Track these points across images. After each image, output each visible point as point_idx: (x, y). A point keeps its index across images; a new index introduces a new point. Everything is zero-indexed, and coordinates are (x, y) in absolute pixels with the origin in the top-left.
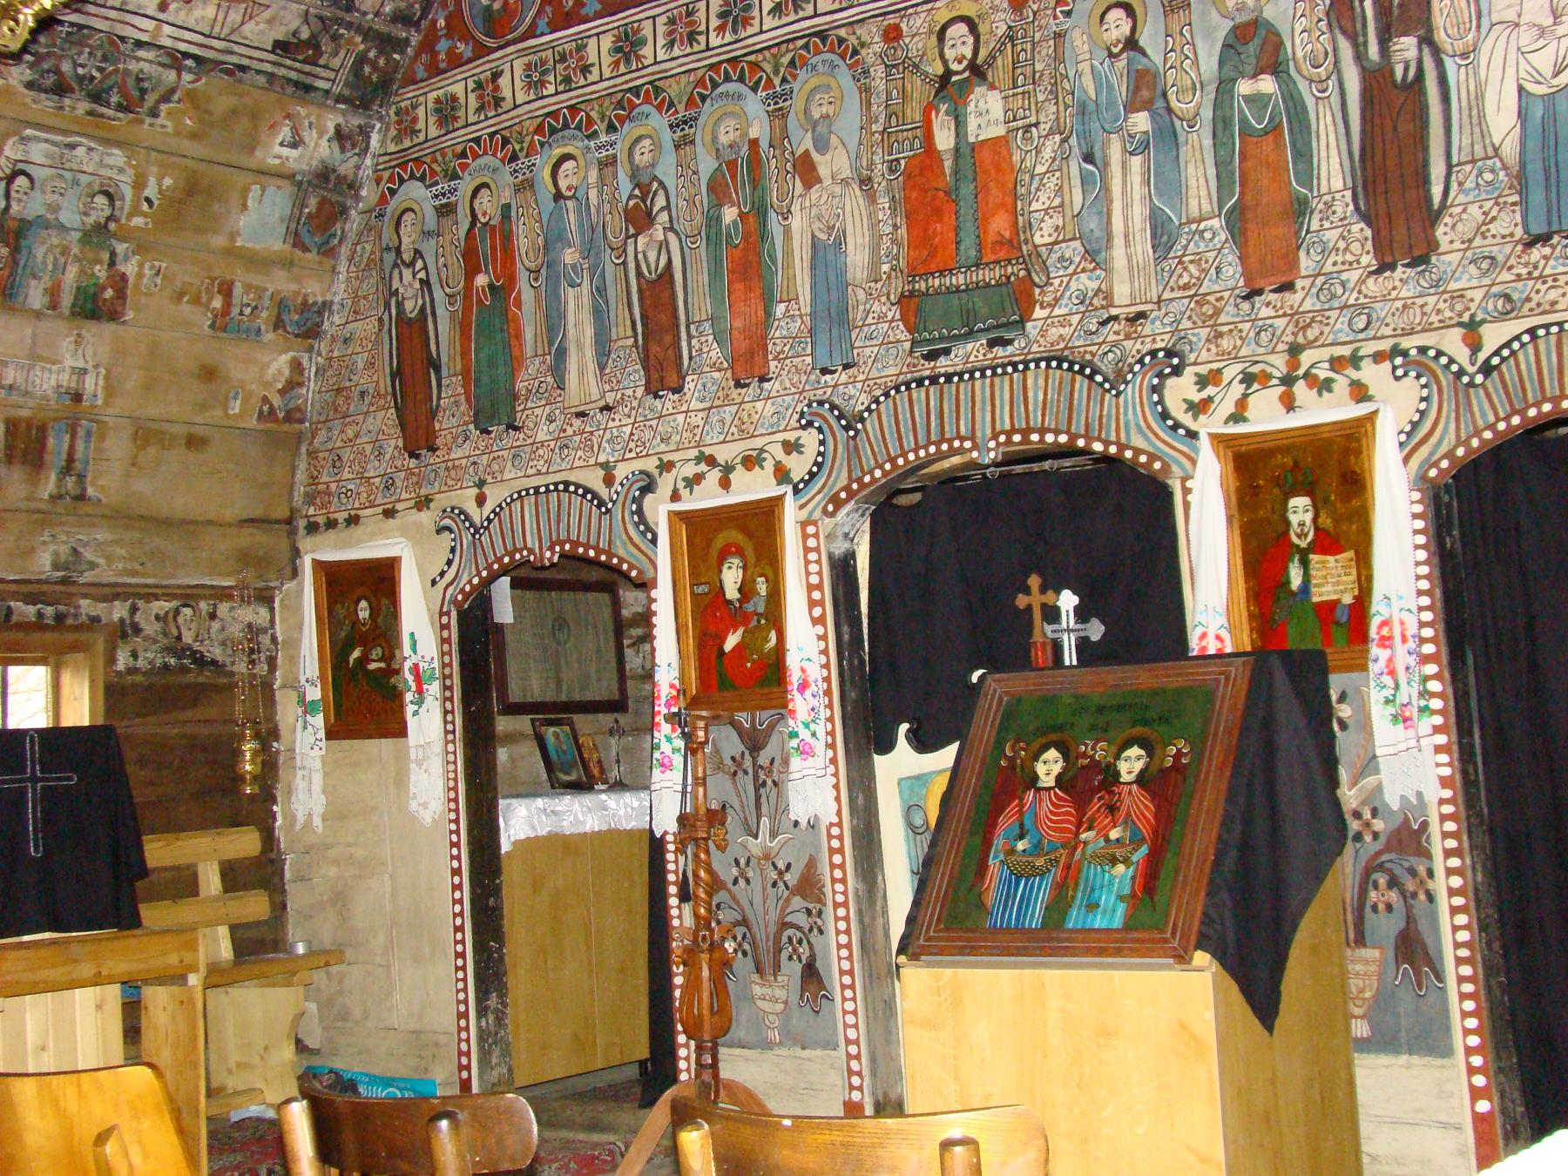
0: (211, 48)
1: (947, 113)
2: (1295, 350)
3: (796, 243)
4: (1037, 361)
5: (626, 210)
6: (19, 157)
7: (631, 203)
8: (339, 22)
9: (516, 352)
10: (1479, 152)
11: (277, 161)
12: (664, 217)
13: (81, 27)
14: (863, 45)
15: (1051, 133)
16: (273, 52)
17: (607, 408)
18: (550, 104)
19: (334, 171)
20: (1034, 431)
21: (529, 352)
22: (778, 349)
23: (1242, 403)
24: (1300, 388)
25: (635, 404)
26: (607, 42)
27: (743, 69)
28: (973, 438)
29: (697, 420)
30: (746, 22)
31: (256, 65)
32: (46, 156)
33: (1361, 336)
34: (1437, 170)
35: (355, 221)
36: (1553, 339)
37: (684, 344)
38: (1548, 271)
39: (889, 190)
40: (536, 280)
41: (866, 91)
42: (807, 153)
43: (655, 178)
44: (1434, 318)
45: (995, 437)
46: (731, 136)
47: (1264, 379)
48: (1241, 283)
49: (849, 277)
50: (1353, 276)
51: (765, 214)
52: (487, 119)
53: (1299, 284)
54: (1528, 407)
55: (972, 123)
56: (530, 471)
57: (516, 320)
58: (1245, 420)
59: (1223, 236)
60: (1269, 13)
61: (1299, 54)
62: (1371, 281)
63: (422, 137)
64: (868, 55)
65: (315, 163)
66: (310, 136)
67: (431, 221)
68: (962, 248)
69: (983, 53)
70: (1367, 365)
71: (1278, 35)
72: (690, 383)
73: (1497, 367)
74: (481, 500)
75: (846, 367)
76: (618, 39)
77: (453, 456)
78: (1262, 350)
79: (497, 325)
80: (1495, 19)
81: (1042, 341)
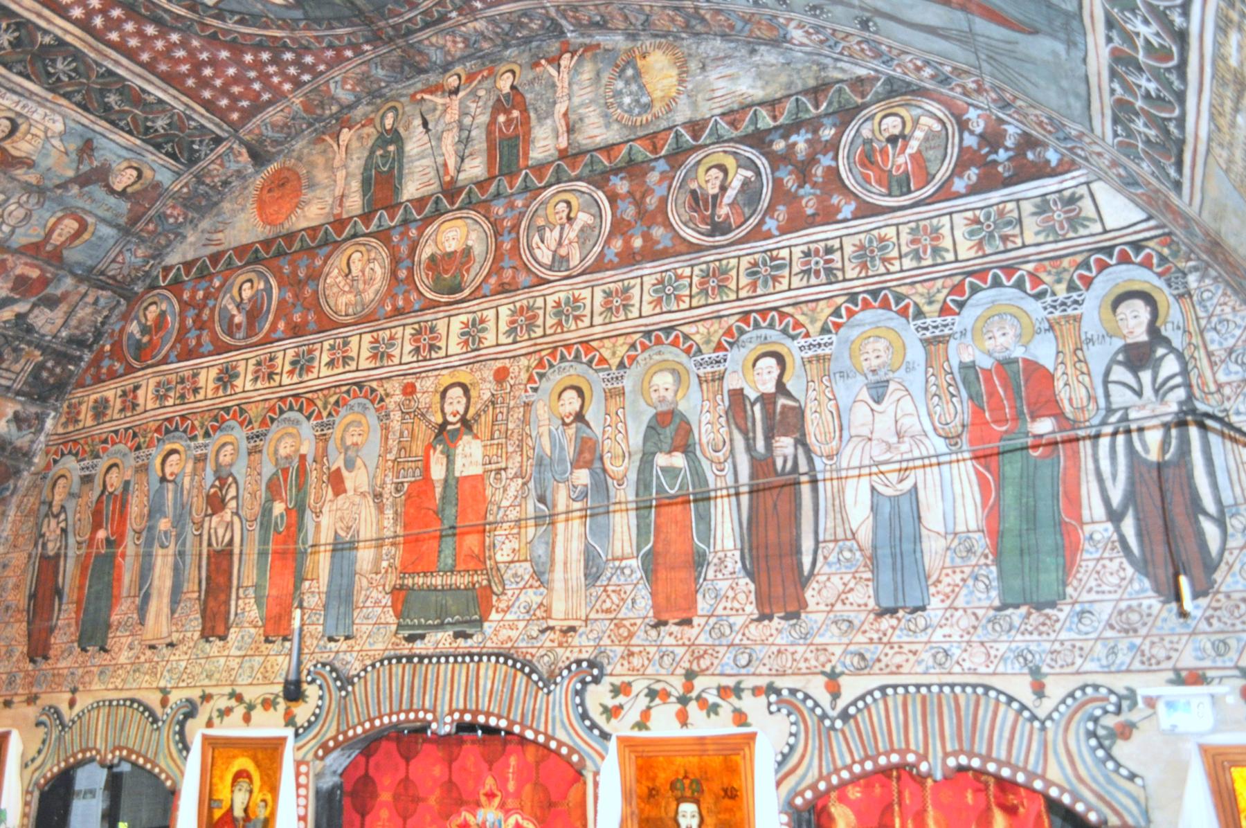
2: (690, 675)
4: (489, 655)
5: (208, 496)
8: (22, 340)
9: (115, 592)
10: (840, 535)
12: (233, 504)
14: (387, 395)
15: (516, 476)
17: (171, 645)
18: (168, 412)
20: (481, 713)
21: (124, 593)
23: (646, 714)
24: (693, 707)
26: (214, 373)
27: (301, 403)
28: (434, 712)
29: (234, 663)
30: (309, 370)
33: (743, 671)
34: (807, 544)
35: (26, 478)
36: (900, 699)
37: (233, 603)
38: (894, 639)
39: (394, 505)
41: (386, 428)
43: (231, 474)
44: (802, 665)
45: (451, 713)
47: (666, 695)
48: (651, 614)
49: (358, 567)
50: (739, 621)
51: (304, 512)
53: (696, 621)
54: (879, 754)
55: (459, 462)
57: (120, 567)
58: (647, 728)
59: (639, 574)
60: (682, 407)
61: (704, 440)
62: (752, 626)
63: (81, 425)
64: (391, 403)
69: (472, 412)
70: (747, 695)
71: (688, 423)
72: (233, 634)
73: (854, 717)
74: (72, 704)
75: (347, 638)
76: (221, 371)
78: (663, 671)
80: (853, 432)
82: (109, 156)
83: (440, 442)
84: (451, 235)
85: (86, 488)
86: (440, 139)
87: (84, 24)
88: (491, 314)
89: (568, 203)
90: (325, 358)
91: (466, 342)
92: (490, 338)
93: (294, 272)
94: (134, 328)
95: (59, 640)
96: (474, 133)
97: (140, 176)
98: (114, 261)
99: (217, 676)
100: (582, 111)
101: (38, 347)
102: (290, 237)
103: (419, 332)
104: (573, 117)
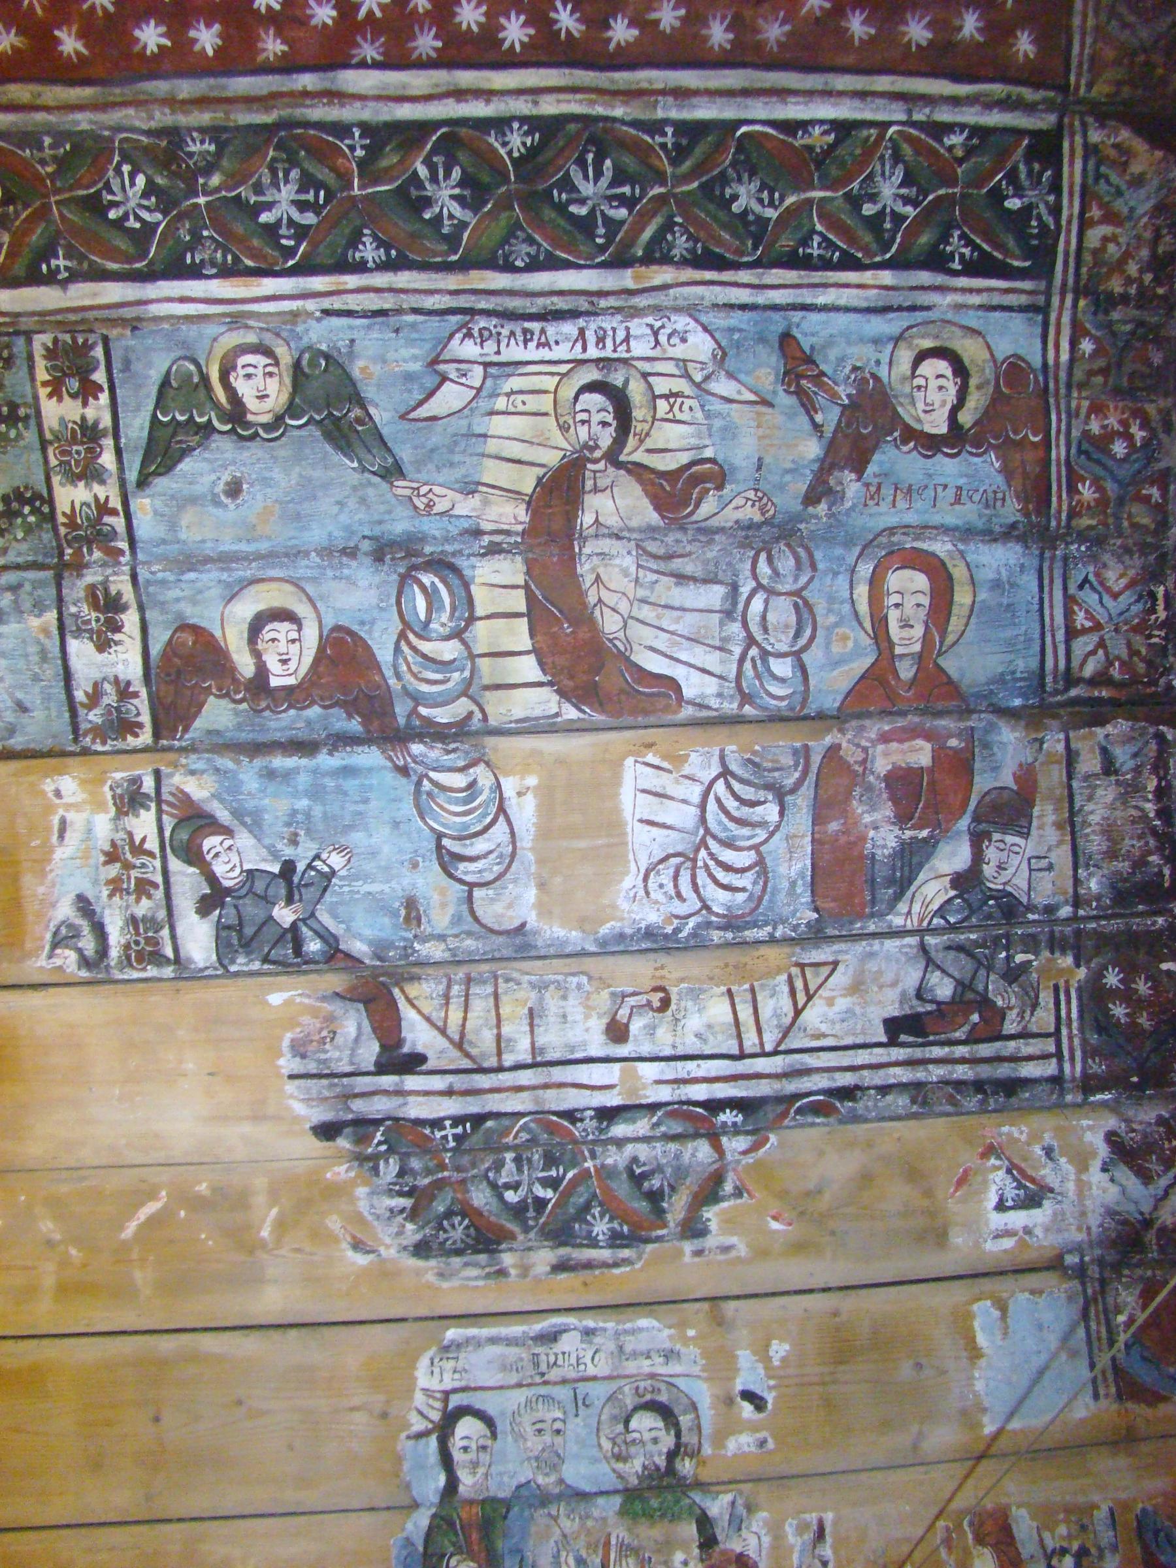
0: (758, 1076)
6: (448, 1384)
11: (1008, 1243)
13: (478, 1119)
16: (892, 1042)
31: (869, 1078)
32: (504, 1368)
65: (1094, 1221)
66: (1058, 1174)
82: (863, 354)
87: (549, 50)
97: (960, 370)
98: (1072, 633)
101: (1056, 944)
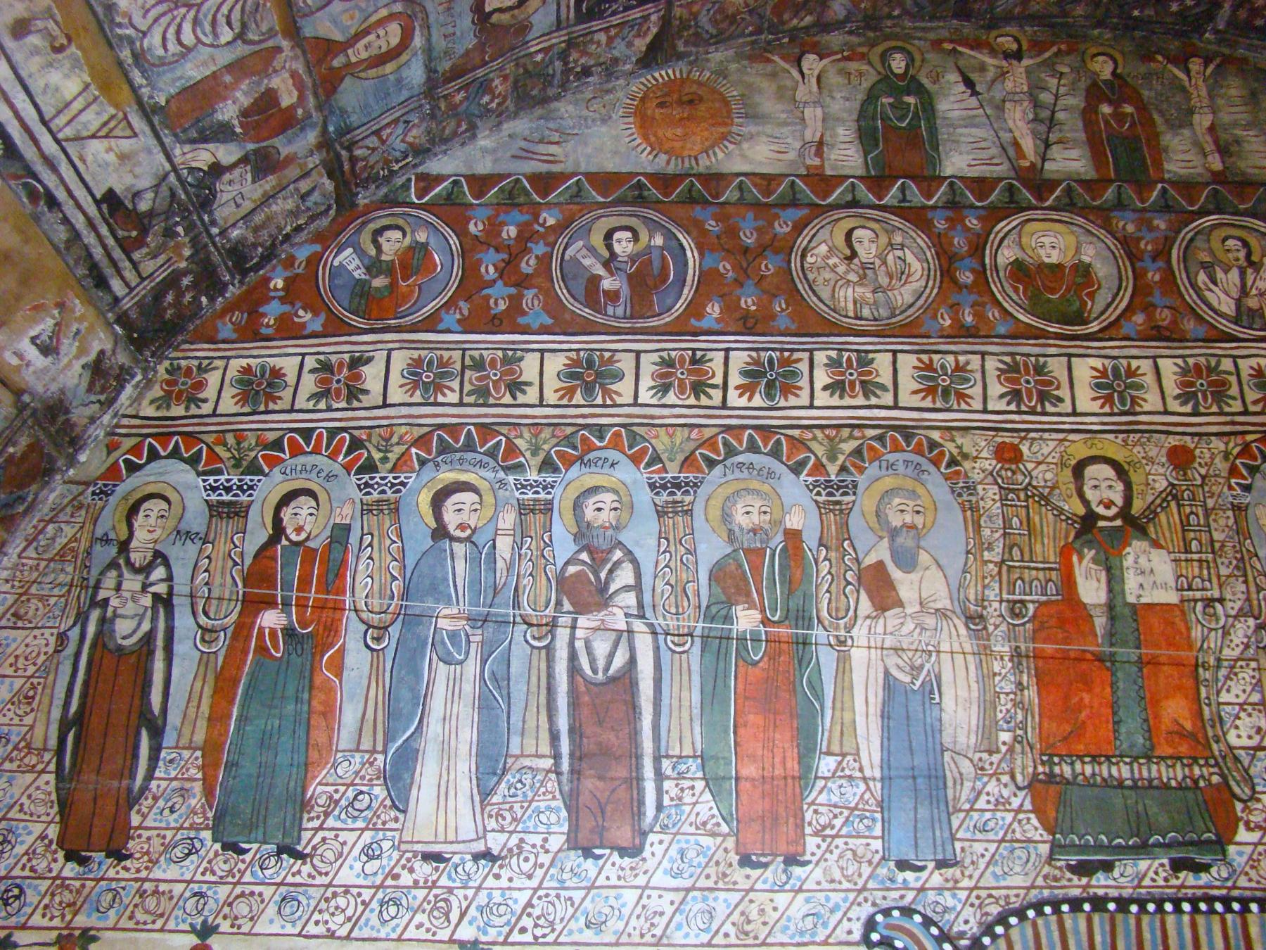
1: (1095, 561)
3: (858, 677)
5: (561, 580)
7: (572, 569)
9: (319, 736)
11: (15, 361)
12: (630, 599)
15: (1241, 614)
16: (98, 203)
17: (487, 855)
19: (67, 411)
21: (345, 738)
22: (823, 820)
25: (545, 859)
26: (556, 364)
27: (786, 446)
30: (787, 390)
35: (55, 493)
40: (378, 639)
41: (972, 511)
42: (881, 564)
46: (755, 518)
49: (947, 739)
52: (329, 409)
55: (1131, 583)
56: (311, 929)
57: (330, 690)
63: (207, 408)
65: (54, 388)
66: (68, 347)
67: (196, 518)
68: (1123, 730)
69: (1137, 506)
75: (941, 864)
76: (577, 363)
77: (157, 873)
79: (291, 690)
81: (1253, 873)
83: (1090, 544)
84: (1046, 240)
85: (225, 527)
86: (1000, 108)
88: (1146, 366)
89: (1245, 244)
90: (822, 378)
91: (1108, 399)
92: (1151, 401)
93: (733, 232)
94: (348, 259)
95: (152, 821)
96: (1060, 116)
98: (377, 133)
99: (615, 925)
100: (1239, 132)
101: (194, 242)
102: (715, 180)
103: (1014, 368)
104: (1224, 136)
